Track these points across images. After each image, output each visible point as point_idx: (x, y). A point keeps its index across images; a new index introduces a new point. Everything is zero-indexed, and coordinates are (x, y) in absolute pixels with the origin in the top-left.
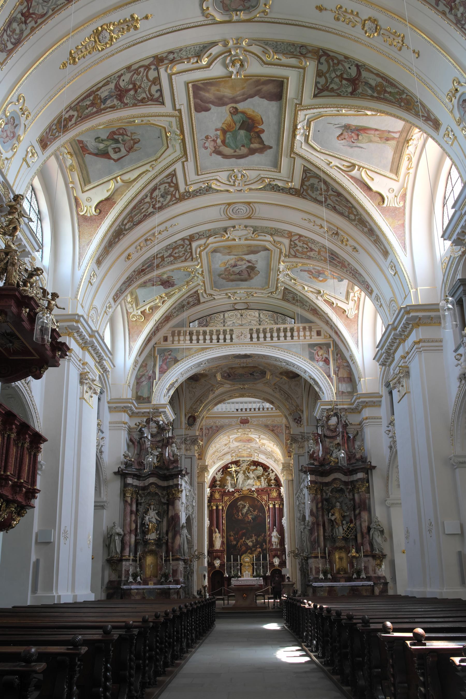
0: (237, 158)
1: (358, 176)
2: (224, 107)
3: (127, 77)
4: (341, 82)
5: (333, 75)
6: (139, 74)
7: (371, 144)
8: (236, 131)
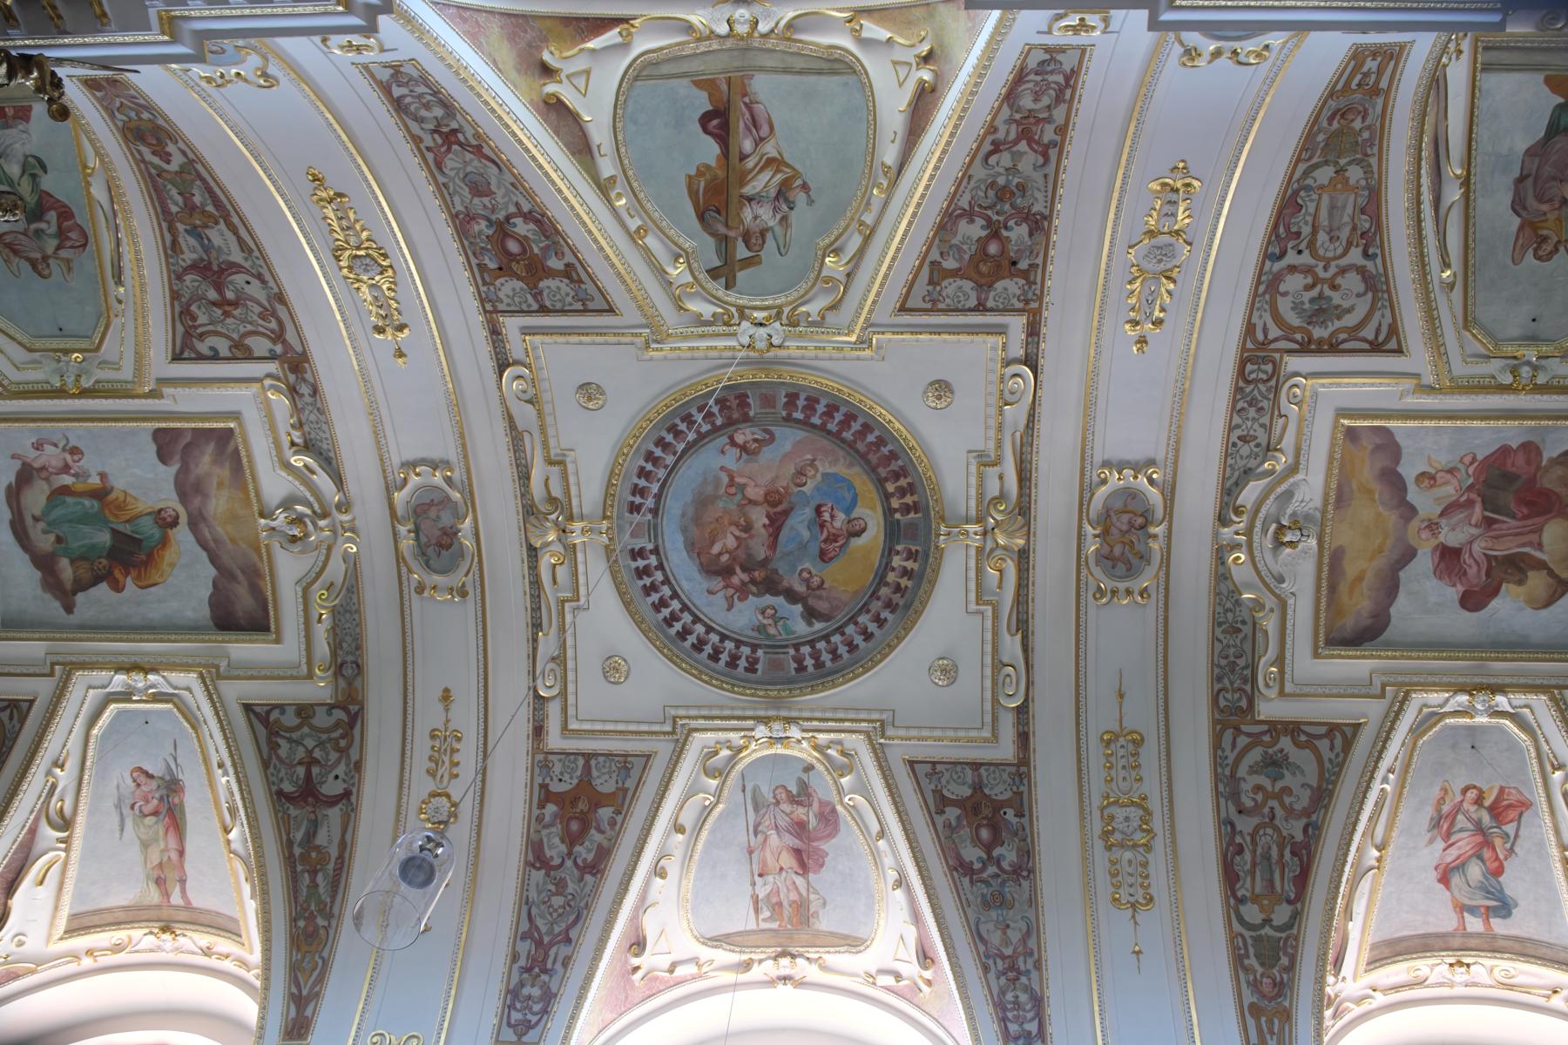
0: (13, 524)
1: (40, 844)
2: (174, 496)
3: (255, 289)
4: (300, 763)
5: (310, 743)
6: (262, 316)
7: (137, 847)
8: (107, 522)
